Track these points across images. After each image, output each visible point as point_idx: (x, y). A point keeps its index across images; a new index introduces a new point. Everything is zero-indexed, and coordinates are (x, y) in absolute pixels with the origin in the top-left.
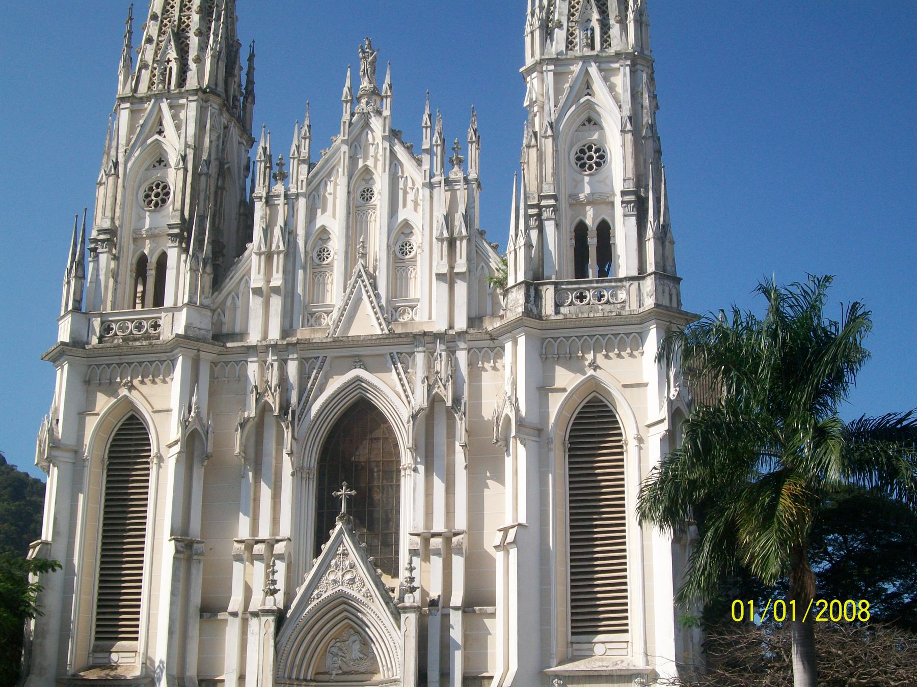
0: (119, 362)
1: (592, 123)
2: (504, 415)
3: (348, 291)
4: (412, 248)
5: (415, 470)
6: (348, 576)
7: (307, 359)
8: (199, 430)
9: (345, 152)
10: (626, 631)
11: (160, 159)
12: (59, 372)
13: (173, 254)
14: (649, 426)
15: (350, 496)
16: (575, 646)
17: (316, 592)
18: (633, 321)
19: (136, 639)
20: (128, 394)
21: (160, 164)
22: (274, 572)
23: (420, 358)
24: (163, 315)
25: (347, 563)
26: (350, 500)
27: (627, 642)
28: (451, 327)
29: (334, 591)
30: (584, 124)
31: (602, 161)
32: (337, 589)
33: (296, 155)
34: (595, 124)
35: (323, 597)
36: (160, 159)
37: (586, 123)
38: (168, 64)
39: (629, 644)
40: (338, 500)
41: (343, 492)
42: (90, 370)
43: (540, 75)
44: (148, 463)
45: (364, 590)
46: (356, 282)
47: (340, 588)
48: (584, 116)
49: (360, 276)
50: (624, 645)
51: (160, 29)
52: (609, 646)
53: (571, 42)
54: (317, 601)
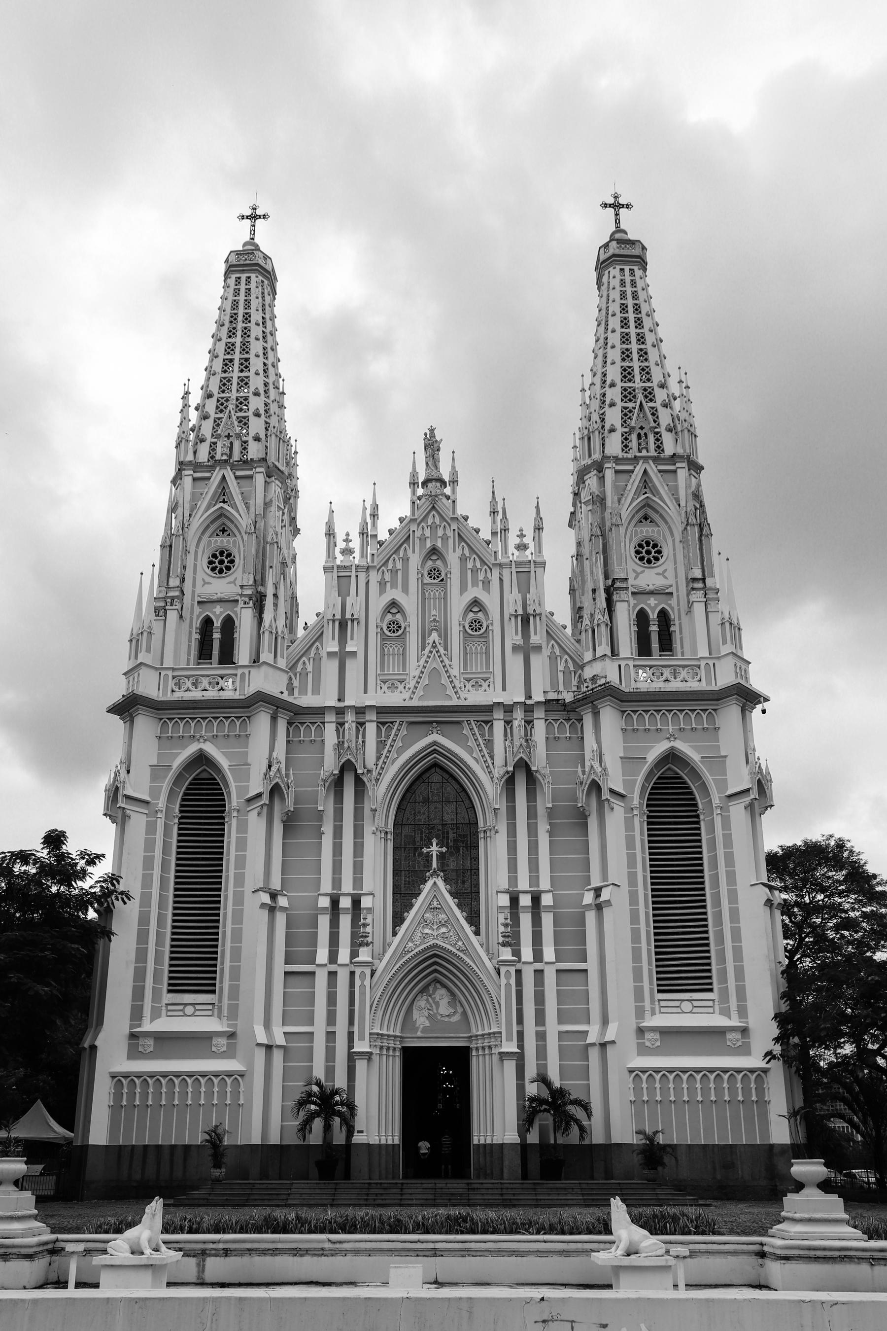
1: (649, 520)
4: (481, 625)
7: (383, 724)
8: (281, 784)
9: (414, 531)
10: (711, 990)
11: (224, 528)
13: (245, 619)
15: (441, 853)
16: (663, 1004)
21: (223, 533)
22: (365, 925)
23: (499, 727)
24: (239, 672)
26: (441, 857)
27: (713, 1000)
28: (530, 697)
30: (641, 522)
31: (659, 556)
32: (431, 943)
34: (651, 522)
36: (224, 528)
37: (643, 520)
38: (228, 439)
40: (429, 857)
41: (435, 849)
43: (598, 473)
46: (431, 652)
48: (641, 514)
49: (434, 647)
51: (217, 407)
52: (695, 1003)
53: (626, 446)
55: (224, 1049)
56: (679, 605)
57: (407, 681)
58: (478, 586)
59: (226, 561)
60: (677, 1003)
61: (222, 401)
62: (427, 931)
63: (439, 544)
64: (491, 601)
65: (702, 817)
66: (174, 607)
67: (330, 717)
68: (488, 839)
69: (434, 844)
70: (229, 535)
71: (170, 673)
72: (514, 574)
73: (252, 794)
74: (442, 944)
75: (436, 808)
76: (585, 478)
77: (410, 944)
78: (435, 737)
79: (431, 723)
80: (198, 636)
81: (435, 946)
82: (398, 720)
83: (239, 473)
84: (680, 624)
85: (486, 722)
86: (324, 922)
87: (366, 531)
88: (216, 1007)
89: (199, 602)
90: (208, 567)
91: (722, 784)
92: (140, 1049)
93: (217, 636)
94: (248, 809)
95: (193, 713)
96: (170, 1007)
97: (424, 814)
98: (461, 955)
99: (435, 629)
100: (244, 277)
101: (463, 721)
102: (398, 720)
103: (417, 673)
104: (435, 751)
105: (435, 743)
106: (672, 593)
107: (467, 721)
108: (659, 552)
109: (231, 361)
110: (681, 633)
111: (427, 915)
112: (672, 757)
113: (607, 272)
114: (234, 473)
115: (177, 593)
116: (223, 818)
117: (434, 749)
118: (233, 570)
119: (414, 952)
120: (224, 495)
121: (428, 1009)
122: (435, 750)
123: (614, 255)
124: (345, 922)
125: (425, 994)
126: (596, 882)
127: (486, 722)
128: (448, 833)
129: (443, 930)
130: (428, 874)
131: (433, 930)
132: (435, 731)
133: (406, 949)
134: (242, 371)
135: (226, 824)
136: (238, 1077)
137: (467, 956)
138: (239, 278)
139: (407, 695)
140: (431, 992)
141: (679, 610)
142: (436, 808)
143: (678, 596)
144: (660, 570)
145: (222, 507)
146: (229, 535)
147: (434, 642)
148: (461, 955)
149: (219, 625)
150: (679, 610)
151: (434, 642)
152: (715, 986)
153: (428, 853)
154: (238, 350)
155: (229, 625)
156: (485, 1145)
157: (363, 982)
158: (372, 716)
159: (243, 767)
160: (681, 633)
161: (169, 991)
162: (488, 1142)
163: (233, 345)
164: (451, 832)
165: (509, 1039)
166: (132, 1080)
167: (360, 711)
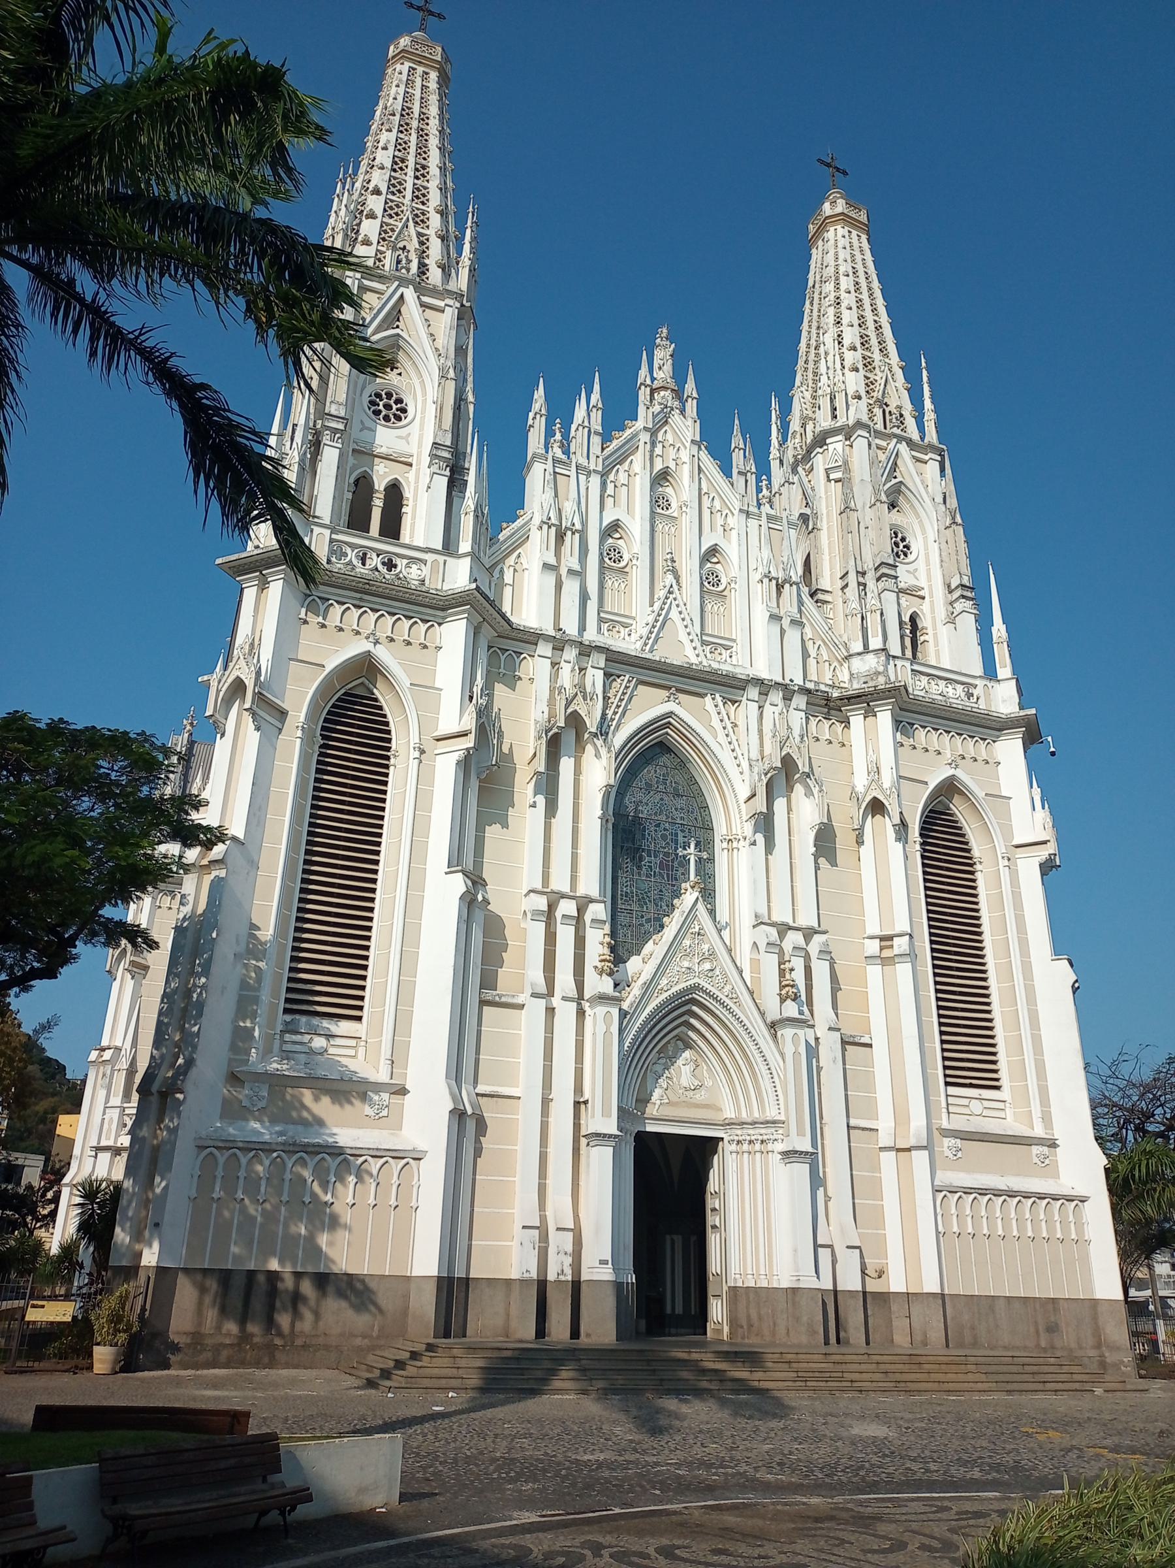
0: (355, 602)
1: (896, 509)
2: (868, 799)
3: (657, 606)
5: (754, 843)
6: (707, 966)
10: (997, 1088)
12: (250, 594)
14: (1018, 846)
17: (664, 982)
18: (993, 724)
19: (359, 1019)
20: (372, 650)
25: (706, 947)
29: (688, 983)
33: (586, 424)
35: (674, 990)
39: (1008, 1105)
42: (307, 602)
44: (388, 758)
45: (728, 988)
46: (667, 598)
47: (696, 980)
50: (1001, 1105)
51: (385, 210)
52: (986, 1104)
54: (666, 995)
56: (933, 611)
57: (634, 627)
59: (394, 407)
60: (965, 1102)
61: (390, 204)
63: (672, 465)
64: (732, 549)
65: (978, 867)
66: (334, 444)
67: (544, 649)
68: (735, 850)
69: (692, 846)
70: (400, 374)
71: (327, 532)
72: (764, 529)
73: (444, 730)
74: (706, 985)
75: (662, 799)
76: (828, 441)
78: (671, 706)
80: (350, 496)
81: (696, 988)
83: (425, 299)
84: (935, 635)
86: (538, 930)
87: (586, 424)
89: (353, 450)
90: (369, 409)
91: (1008, 831)
93: (378, 503)
94: (437, 752)
95: (361, 599)
97: (647, 804)
98: (731, 1005)
100: (420, 70)
102: (628, 676)
103: (651, 619)
105: (670, 714)
106: (923, 598)
108: (907, 547)
109: (403, 161)
110: (936, 645)
112: (950, 788)
113: (832, 229)
114: (418, 297)
115: (341, 427)
116: (388, 758)
117: (664, 722)
118: (404, 422)
119: (670, 992)
120: (398, 320)
123: (842, 214)
124: (565, 936)
125: (662, 1055)
126: (873, 928)
128: (676, 835)
129: (707, 966)
130: (683, 885)
133: (659, 987)
134: (417, 178)
135: (392, 768)
138: (414, 69)
139: (639, 645)
140: (670, 1053)
141: (934, 619)
142: (662, 799)
143: (932, 602)
144: (910, 567)
145: (398, 335)
146: (400, 374)
147: (671, 586)
149: (382, 489)
150: (934, 619)
151: (671, 586)
152: (1005, 1082)
153: (684, 857)
154: (413, 150)
155: (394, 492)
156: (757, 1290)
158: (600, 660)
159: (426, 689)
160: (936, 645)
162: (764, 1284)
163: (405, 143)
164: (680, 835)
165: (800, 1133)
166: (235, 1154)
167: (586, 650)
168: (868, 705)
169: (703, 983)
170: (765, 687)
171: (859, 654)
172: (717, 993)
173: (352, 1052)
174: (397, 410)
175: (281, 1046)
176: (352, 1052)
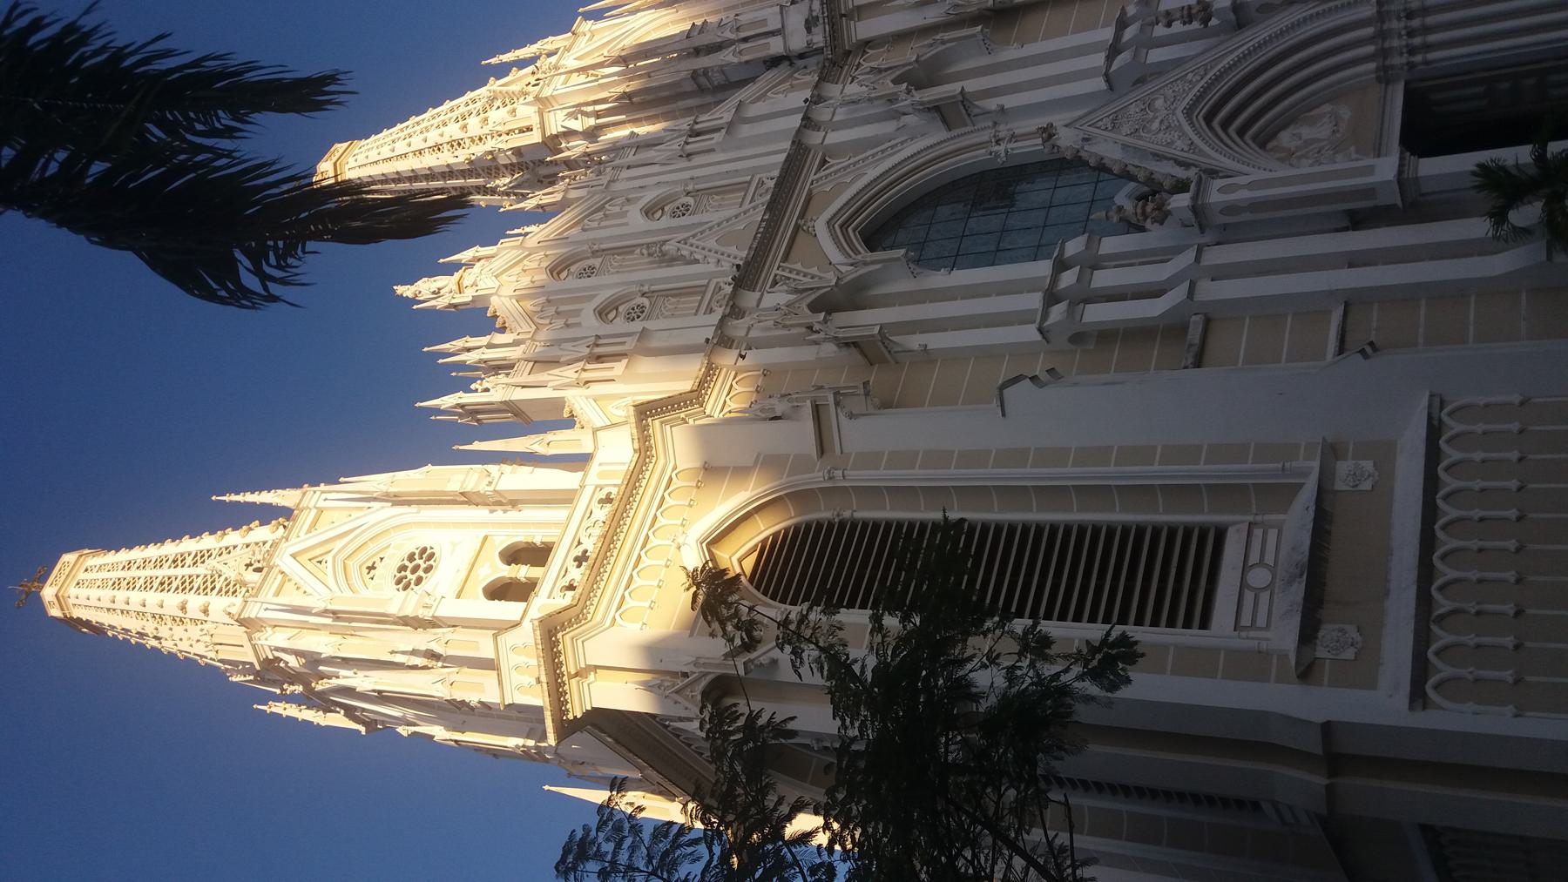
55: (1368, 465)
58: (627, 211)
62: (1155, 125)
70: (382, 559)
77: (1179, 143)
79: (797, 228)
81: (1189, 112)
82: (775, 271)
85: (824, 162)
88: (1259, 518)
92: (1349, 654)
96: (1246, 620)
99: (662, 246)
101: (810, 190)
104: (844, 226)
107: (812, 184)
111: (1126, 129)
121: (1319, 152)
122: (841, 227)
127: (824, 162)
129: (1159, 103)
131: (1155, 118)
132: (810, 224)
136: (1446, 410)
137: (1216, 65)
148: (1210, 74)
157: (1243, 187)
161: (1204, 625)
168: (844, 15)
169: (1184, 104)
170: (808, 122)
171: (784, 38)
172: (1198, 87)
173: (1272, 535)
174: (421, 558)
175: (1261, 629)
176: (1272, 535)
